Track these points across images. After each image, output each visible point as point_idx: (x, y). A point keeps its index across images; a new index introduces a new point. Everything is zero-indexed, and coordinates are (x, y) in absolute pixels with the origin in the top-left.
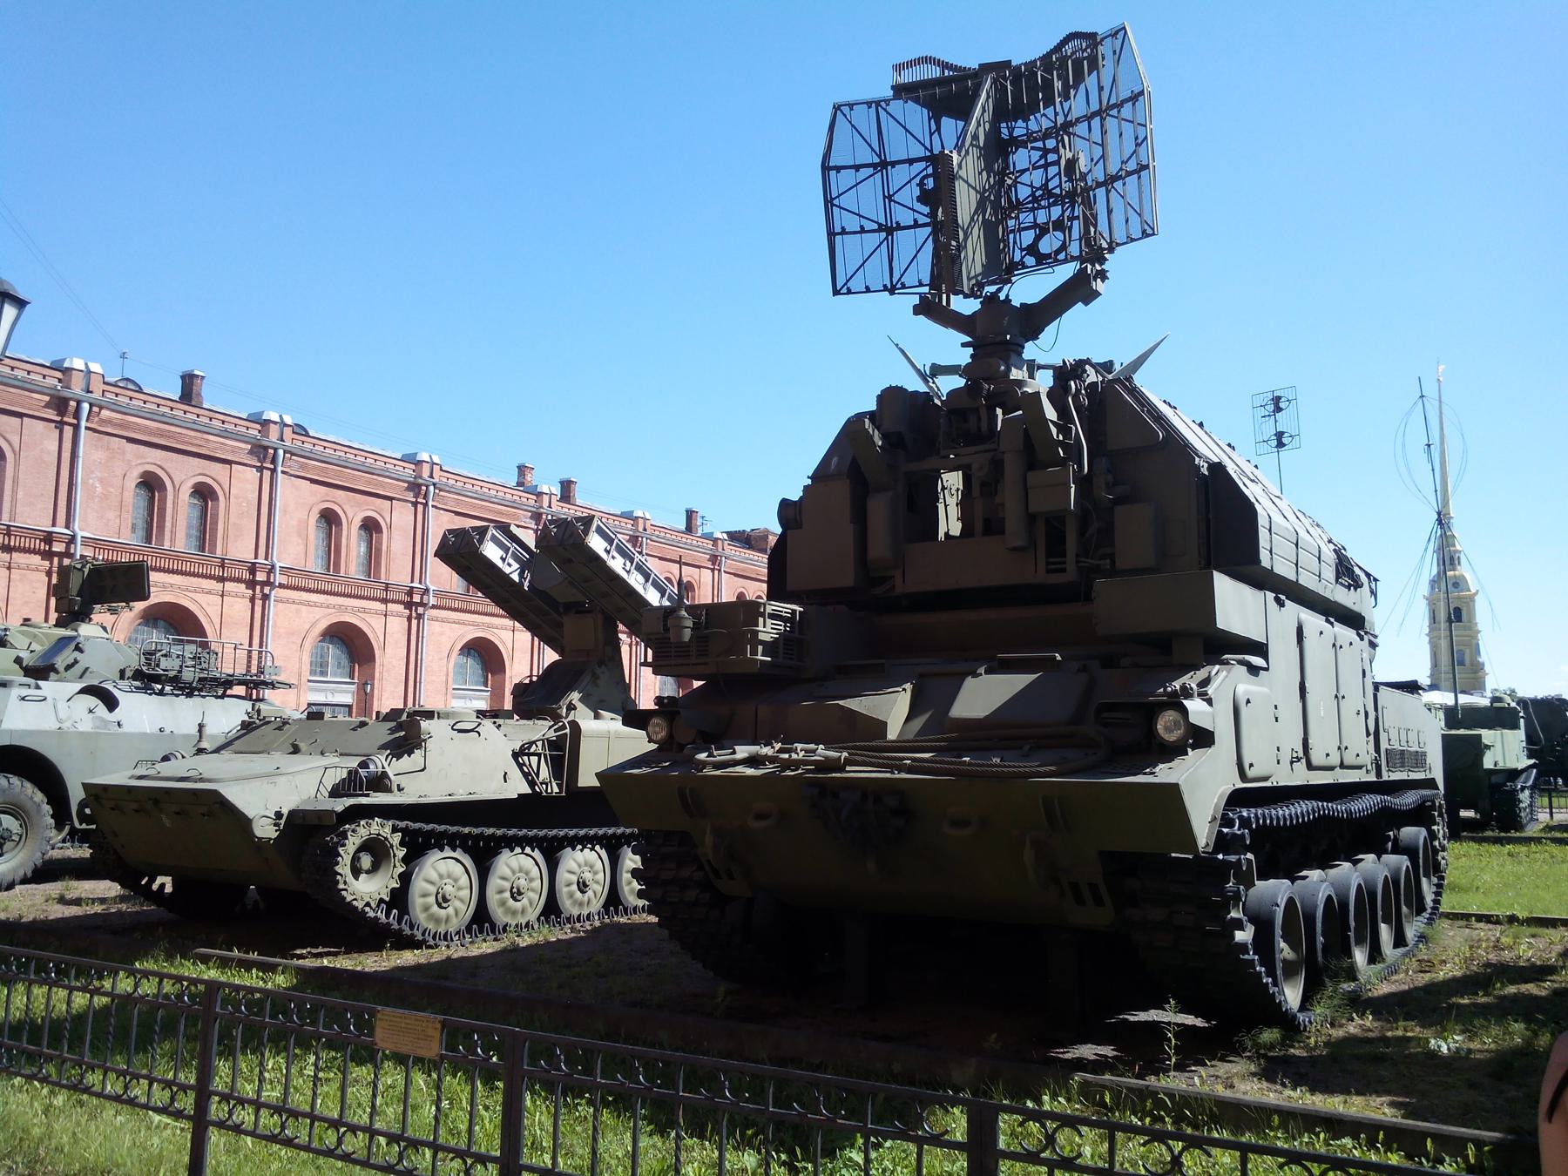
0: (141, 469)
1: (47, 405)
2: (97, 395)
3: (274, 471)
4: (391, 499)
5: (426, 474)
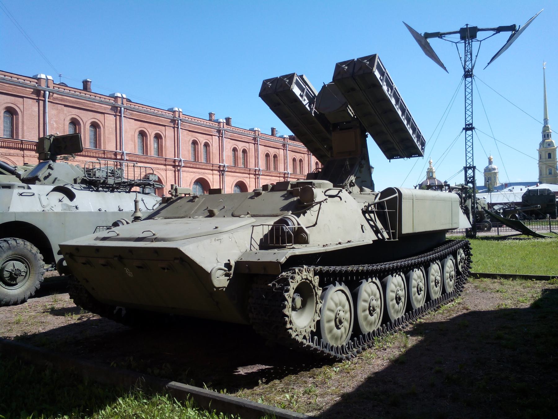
1: (33, 93)
2: (51, 88)
3: (120, 116)
4: (165, 126)
5: (177, 116)
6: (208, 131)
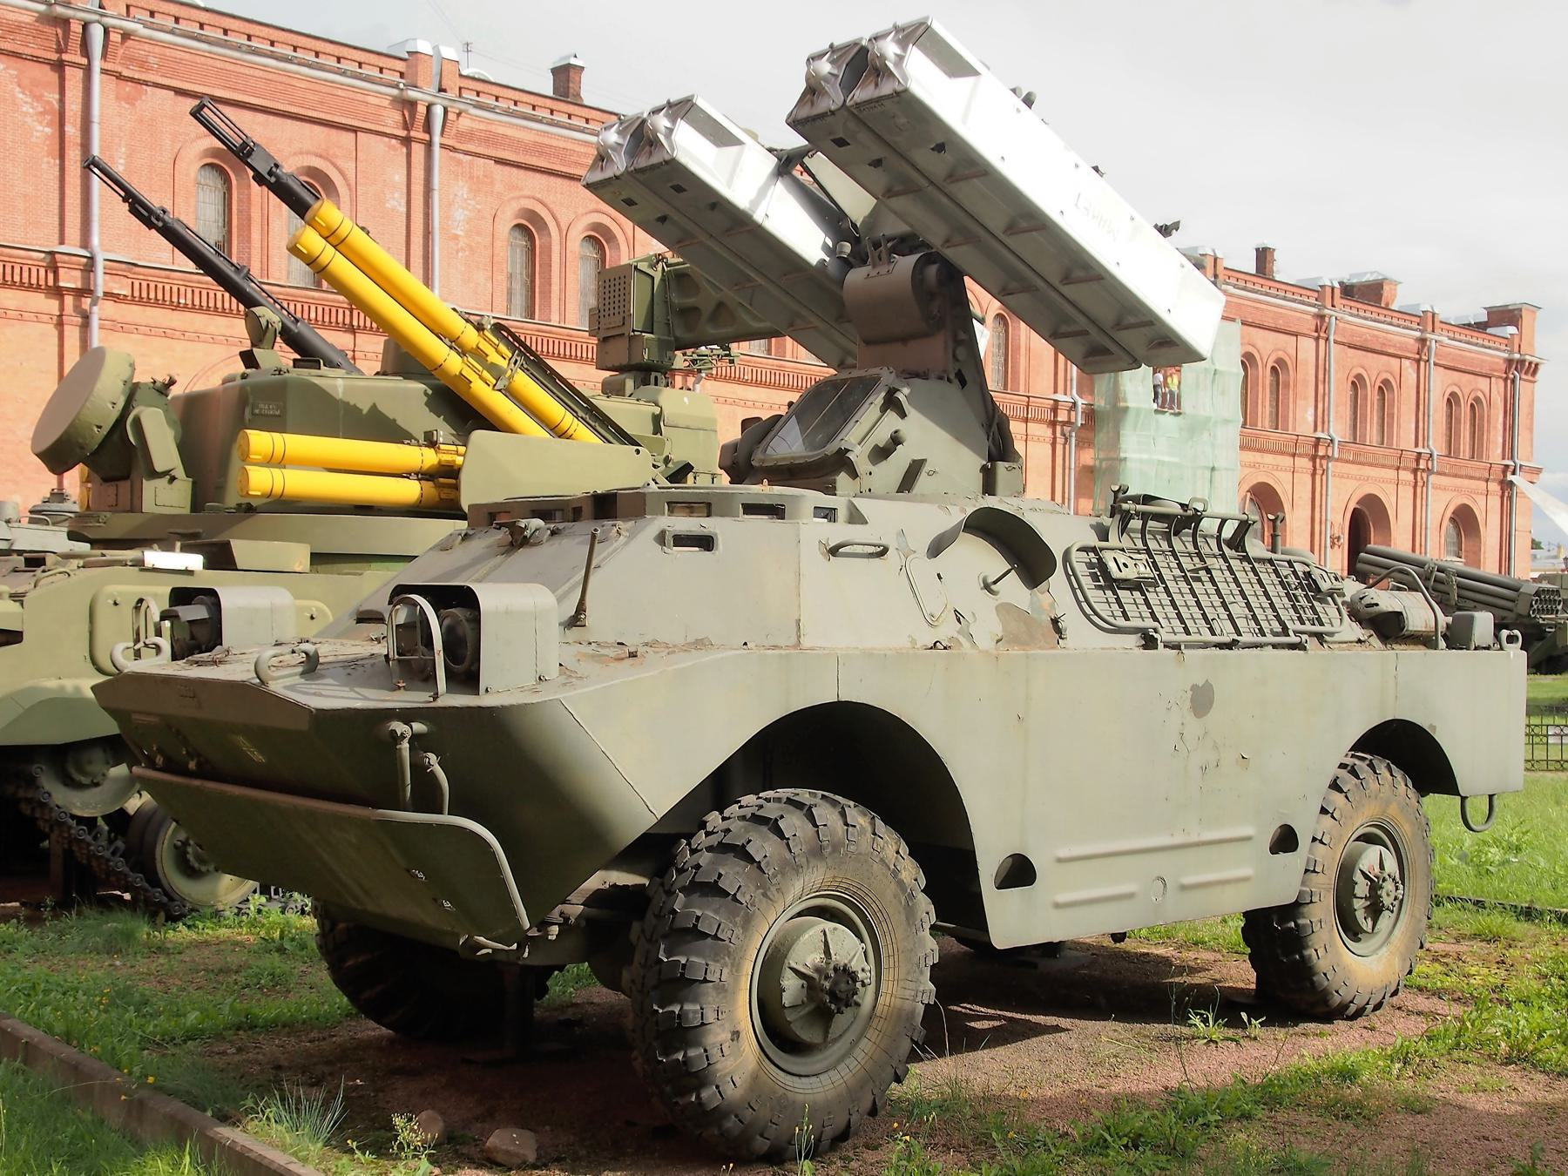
0: (515, 206)
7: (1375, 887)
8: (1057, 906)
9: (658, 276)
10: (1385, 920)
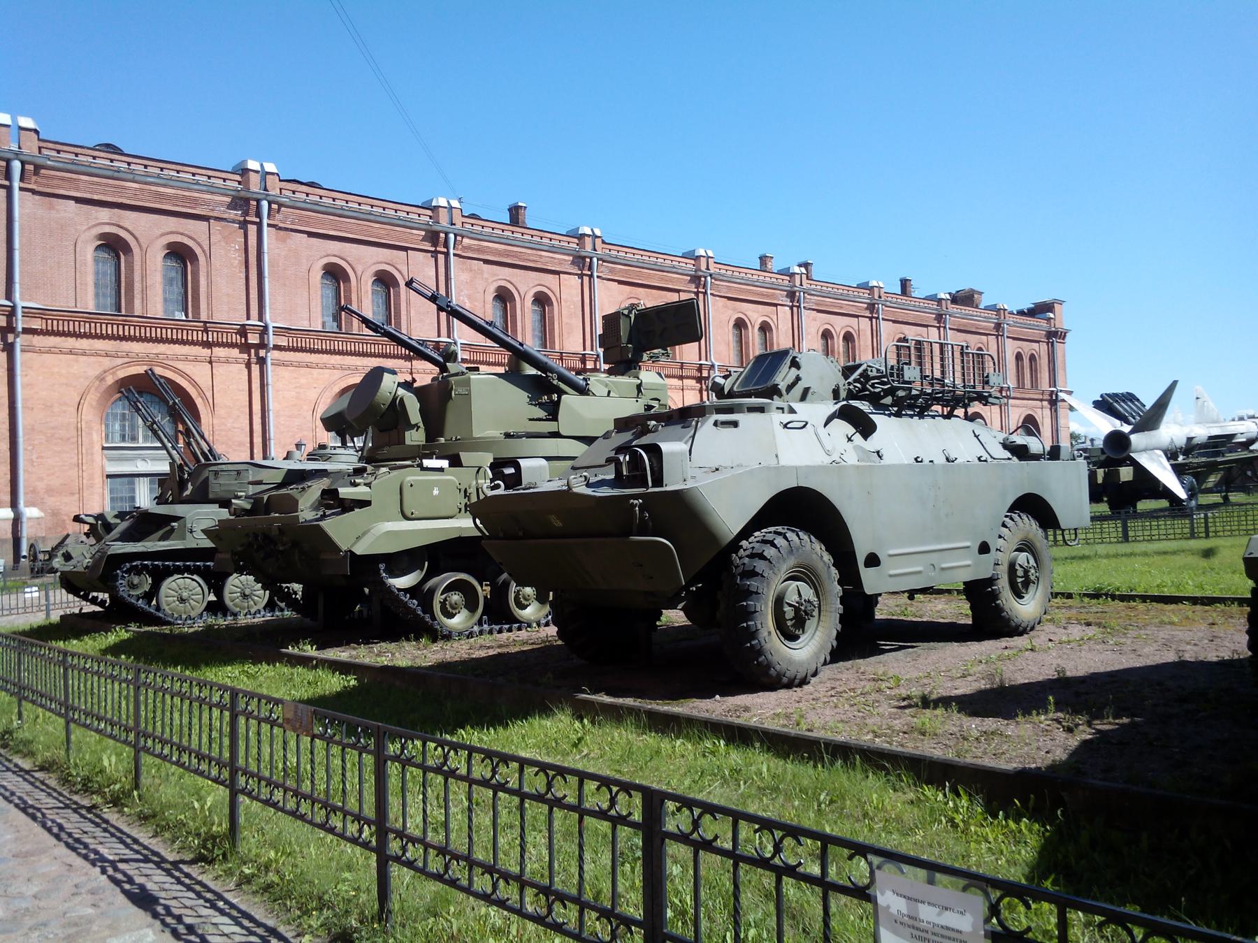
0: (496, 285)
3: (591, 276)
5: (703, 267)
6: (767, 296)
7: (1026, 572)
8: (891, 576)
9: (632, 316)
10: (1032, 588)
